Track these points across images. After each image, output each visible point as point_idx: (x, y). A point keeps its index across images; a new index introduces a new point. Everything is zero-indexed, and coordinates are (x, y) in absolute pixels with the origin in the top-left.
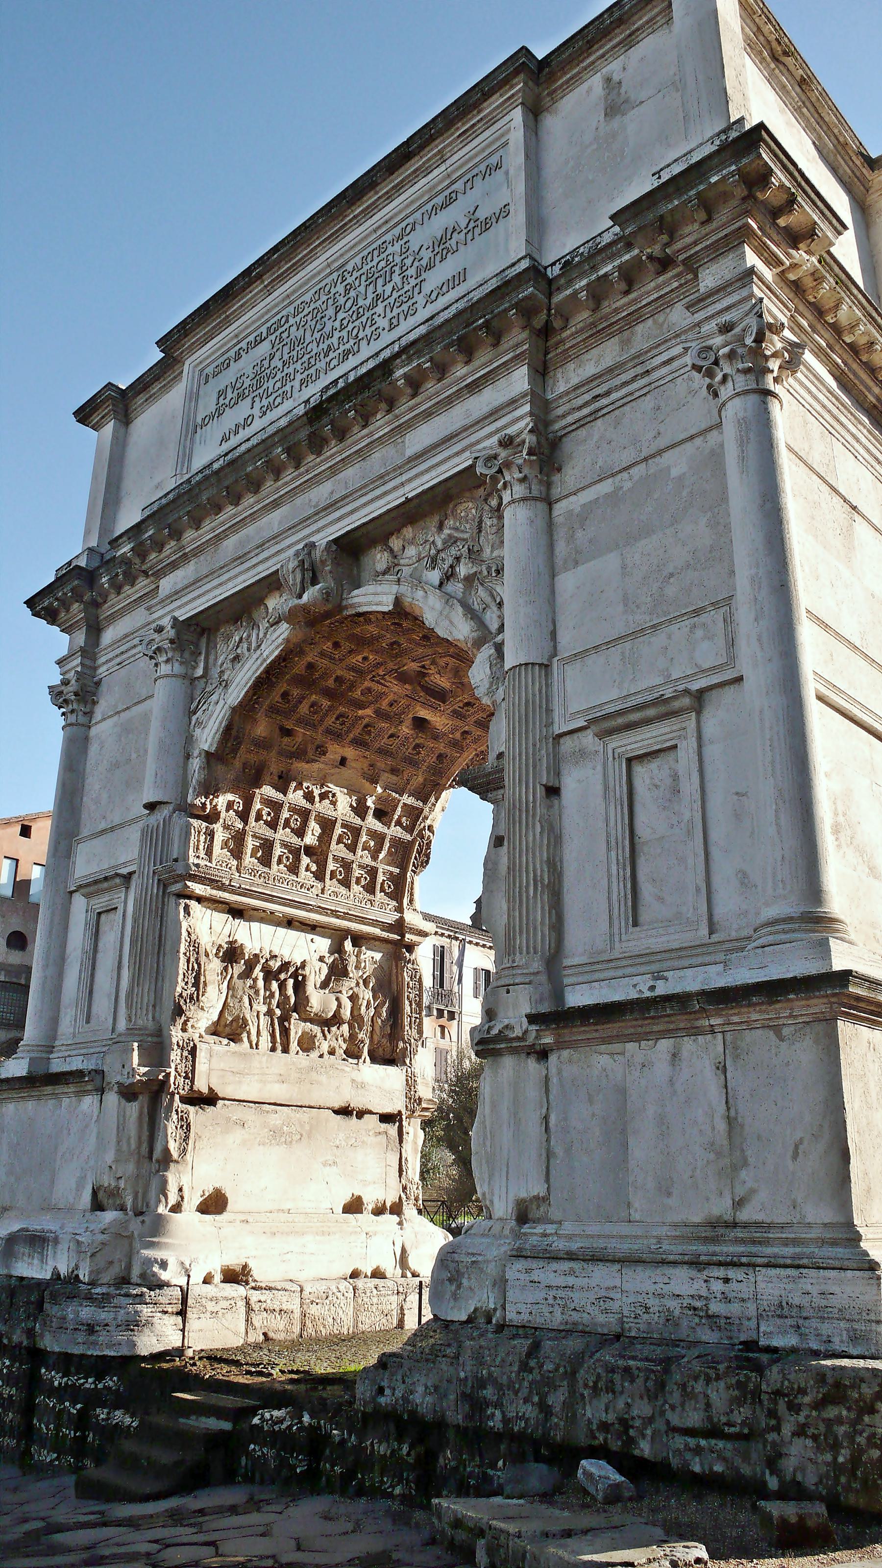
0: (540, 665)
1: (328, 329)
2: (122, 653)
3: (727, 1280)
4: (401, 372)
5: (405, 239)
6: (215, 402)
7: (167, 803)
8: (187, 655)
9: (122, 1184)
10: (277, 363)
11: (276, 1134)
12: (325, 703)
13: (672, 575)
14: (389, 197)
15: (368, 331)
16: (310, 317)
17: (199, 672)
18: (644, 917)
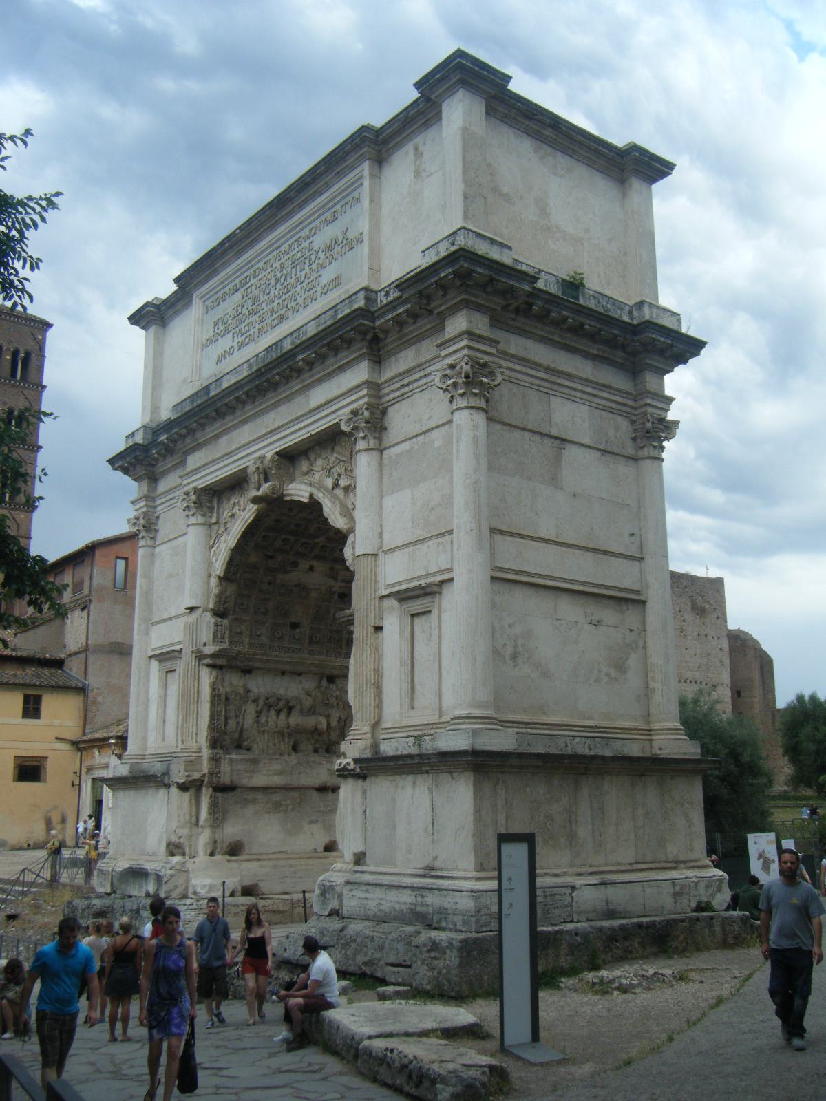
0: (372, 555)
1: (272, 295)
2: (170, 500)
3: (422, 896)
4: (300, 357)
5: (311, 239)
6: (212, 330)
7: (198, 608)
8: (205, 509)
9: (182, 840)
10: (245, 311)
11: (277, 806)
12: (292, 538)
13: (433, 509)
14: (301, 206)
15: (293, 304)
16: (262, 282)
17: (214, 520)
18: (416, 704)
